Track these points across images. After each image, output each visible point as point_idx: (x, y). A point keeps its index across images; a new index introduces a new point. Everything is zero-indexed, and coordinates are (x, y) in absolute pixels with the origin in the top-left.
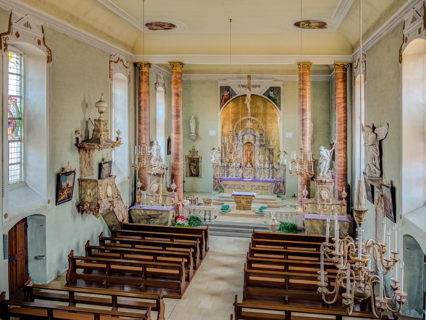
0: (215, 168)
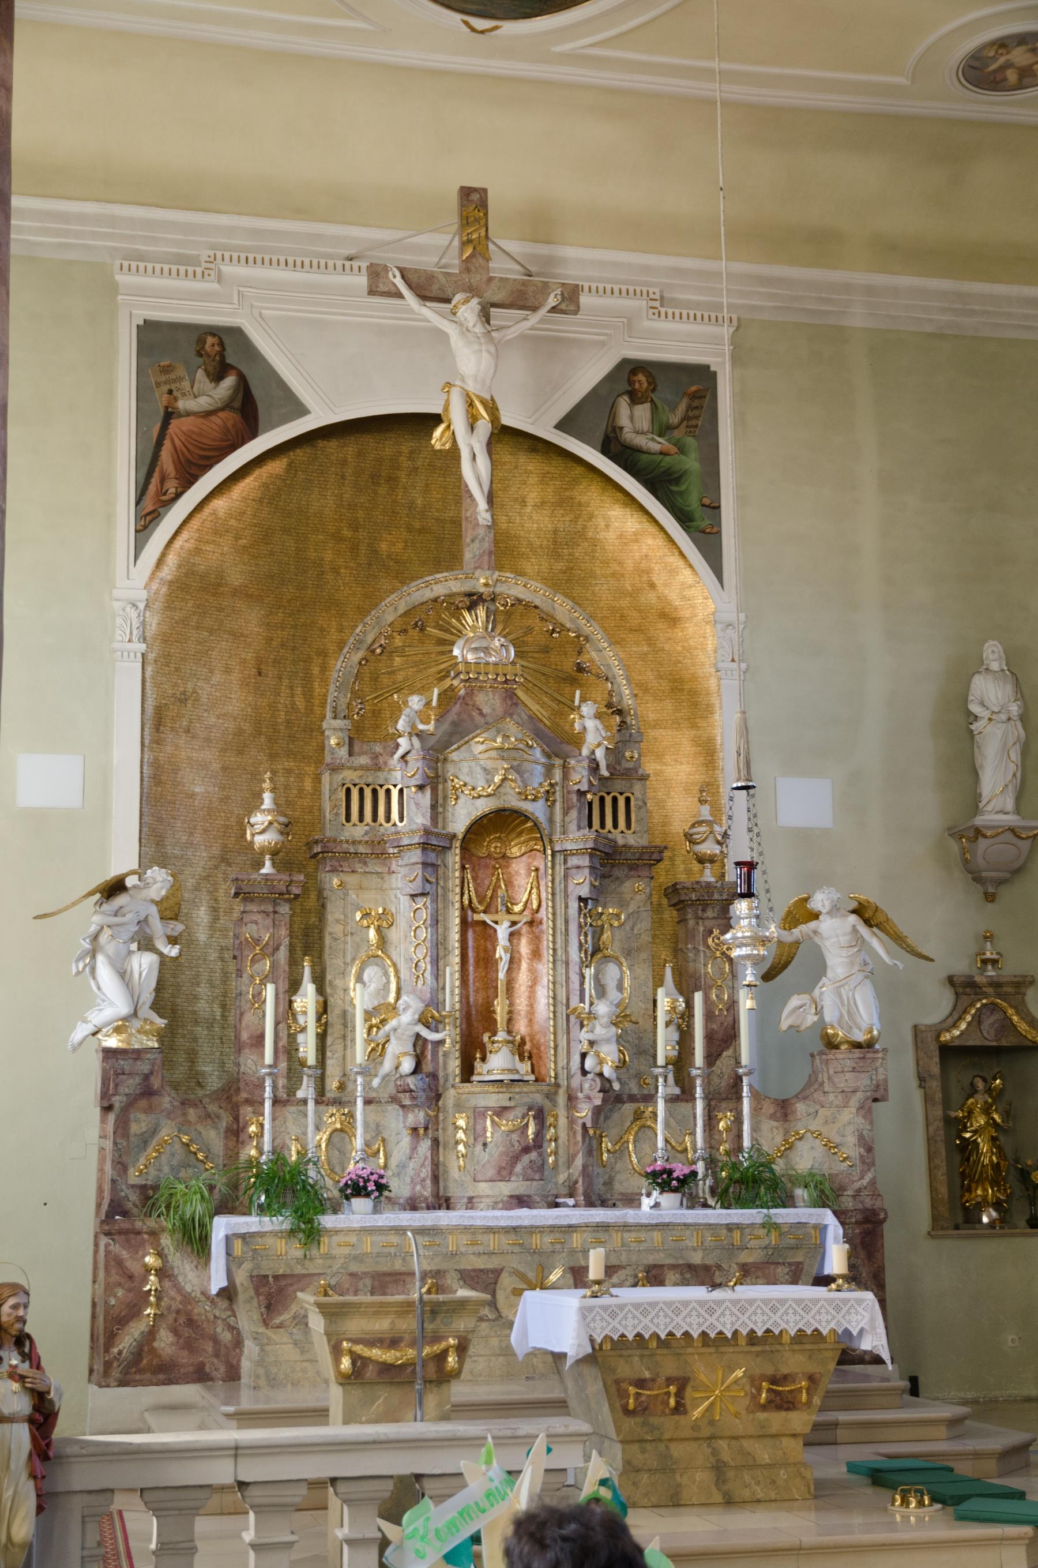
0: (126, 1109)
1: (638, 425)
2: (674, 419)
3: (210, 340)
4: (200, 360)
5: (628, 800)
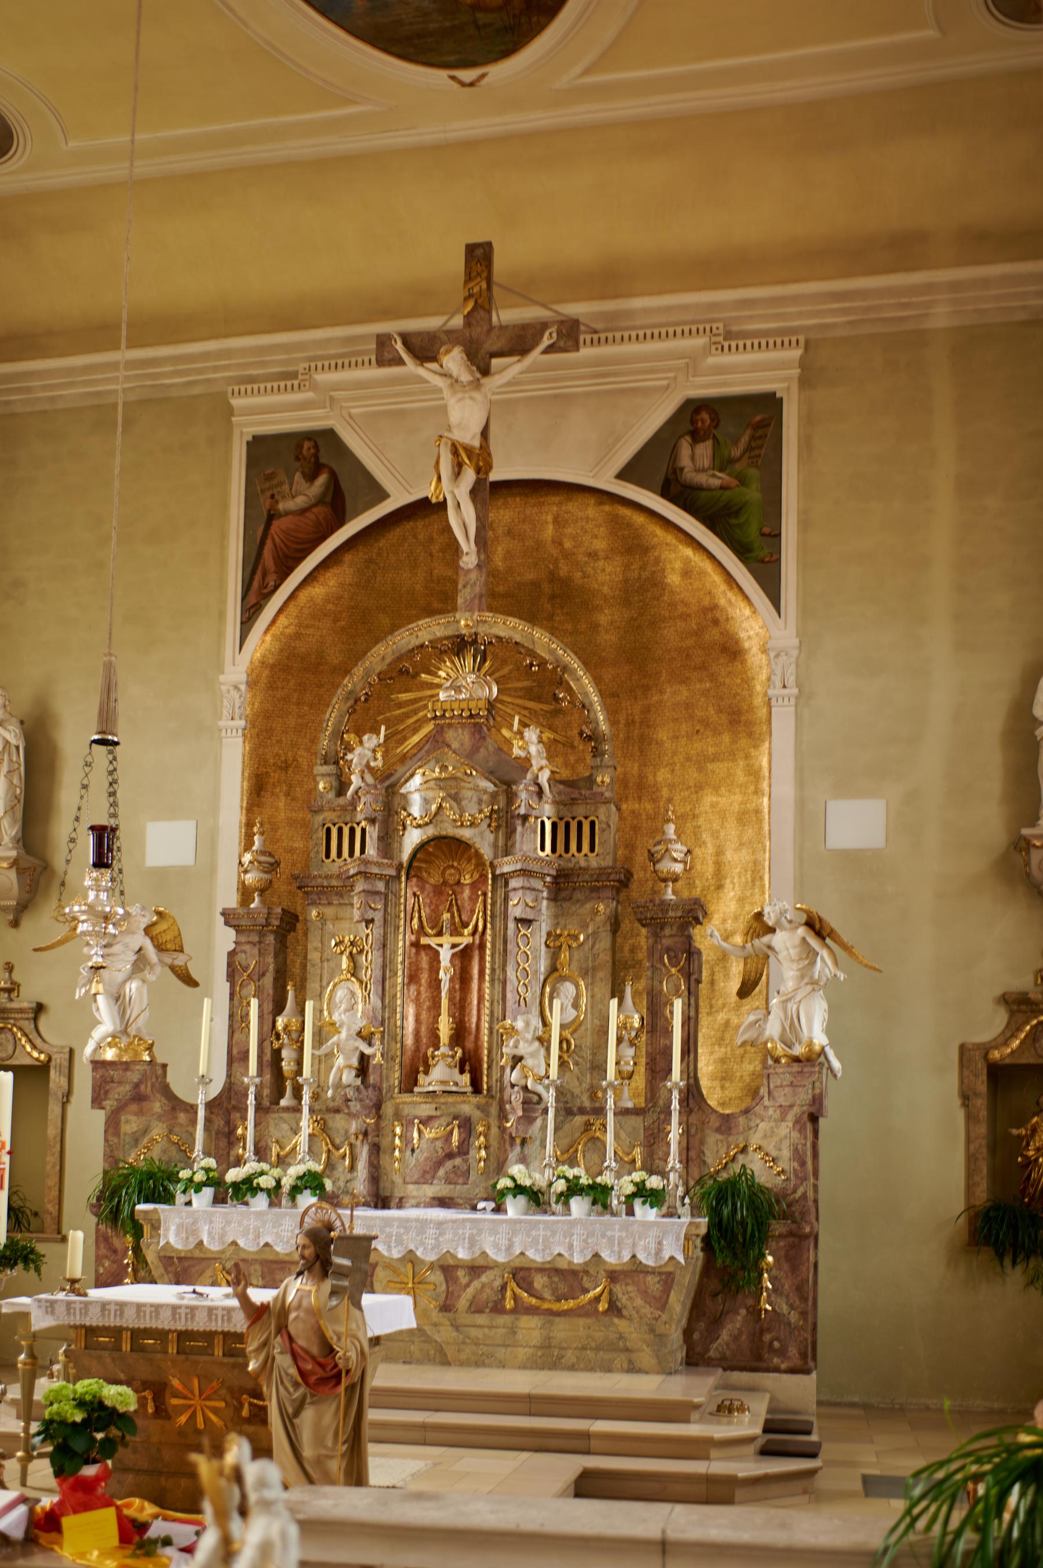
1: (699, 464)
2: (736, 452)
3: (307, 444)
4: (298, 464)
5: (592, 824)
